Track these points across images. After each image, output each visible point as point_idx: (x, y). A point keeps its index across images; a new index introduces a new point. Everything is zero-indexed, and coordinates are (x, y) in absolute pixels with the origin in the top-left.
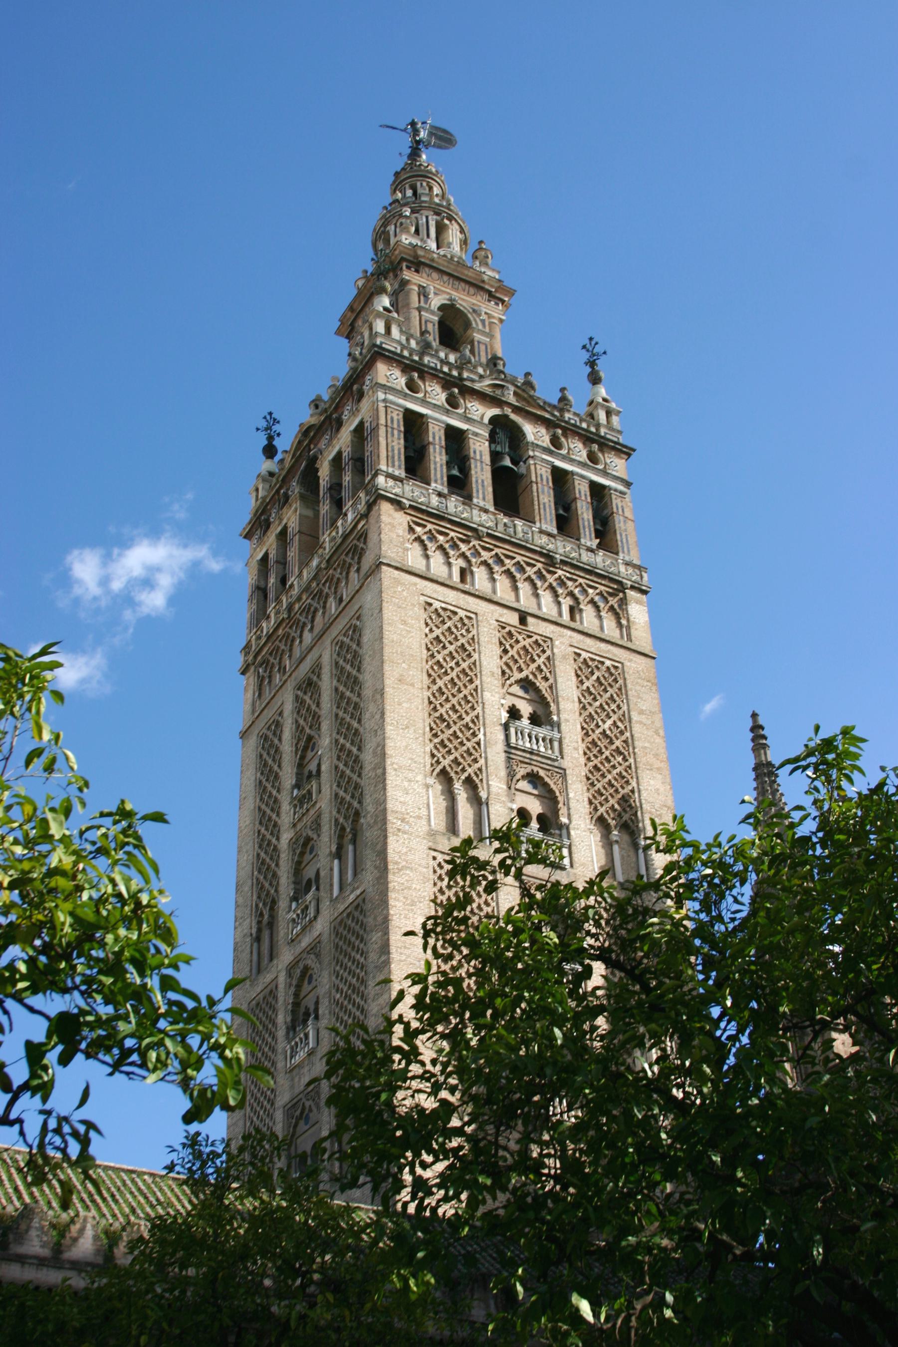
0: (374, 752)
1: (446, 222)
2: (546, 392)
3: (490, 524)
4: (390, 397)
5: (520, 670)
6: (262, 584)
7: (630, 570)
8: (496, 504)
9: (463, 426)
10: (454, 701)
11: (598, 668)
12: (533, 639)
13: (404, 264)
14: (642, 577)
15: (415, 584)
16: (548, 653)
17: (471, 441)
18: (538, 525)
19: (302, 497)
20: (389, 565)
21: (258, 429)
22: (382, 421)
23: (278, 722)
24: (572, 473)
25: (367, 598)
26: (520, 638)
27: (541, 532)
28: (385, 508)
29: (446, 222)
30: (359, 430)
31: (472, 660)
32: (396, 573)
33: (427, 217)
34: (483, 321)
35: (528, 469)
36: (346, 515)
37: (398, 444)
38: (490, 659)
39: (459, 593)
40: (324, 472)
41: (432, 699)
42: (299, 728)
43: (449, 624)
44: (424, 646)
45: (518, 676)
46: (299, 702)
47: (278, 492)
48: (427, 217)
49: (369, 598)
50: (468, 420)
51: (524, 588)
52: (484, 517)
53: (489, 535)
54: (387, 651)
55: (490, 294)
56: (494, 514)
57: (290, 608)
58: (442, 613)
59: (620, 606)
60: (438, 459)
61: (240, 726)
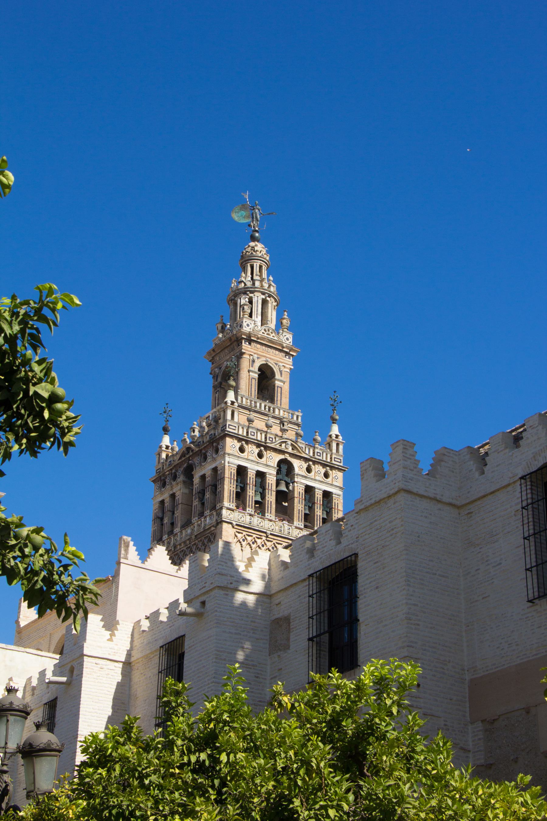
1: (268, 299)
3: (273, 527)
6: (160, 515)
13: (243, 341)
17: (267, 479)
19: (184, 482)
27: (296, 528)
29: (268, 299)
30: (215, 470)
35: (294, 487)
36: (206, 517)
40: (196, 480)
47: (171, 470)
53: (271, 534)
56: (275, 522)
60: (251, 493)
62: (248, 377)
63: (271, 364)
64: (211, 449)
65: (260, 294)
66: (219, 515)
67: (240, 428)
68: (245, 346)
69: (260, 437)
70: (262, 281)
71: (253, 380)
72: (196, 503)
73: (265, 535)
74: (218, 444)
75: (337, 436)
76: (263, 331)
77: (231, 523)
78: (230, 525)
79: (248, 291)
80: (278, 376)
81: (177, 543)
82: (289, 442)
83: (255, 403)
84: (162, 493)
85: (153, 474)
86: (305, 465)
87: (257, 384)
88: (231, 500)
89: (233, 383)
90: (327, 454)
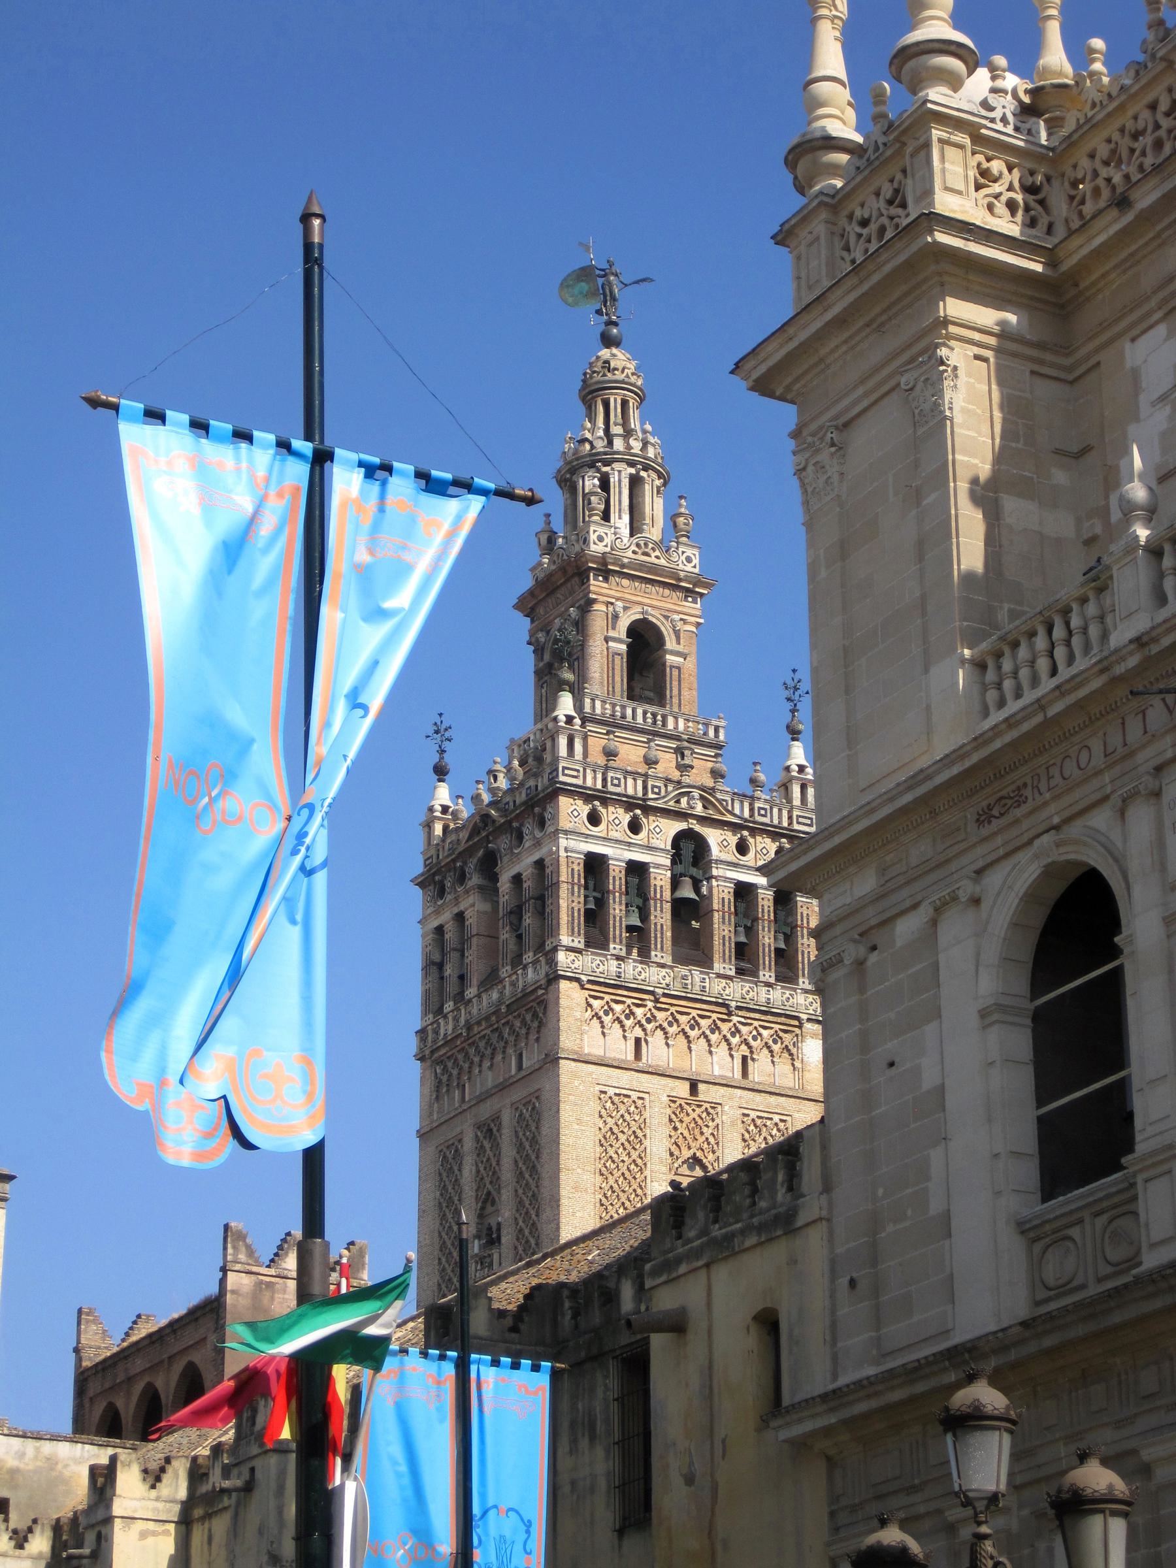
1: (643, 474)
3: (668, 980)
4: (572, 844)
6: (437, 957)
12: (703, 1108)
15: (591, 1074)
16: (717, 1121)
17: (652, 875)
19: (481, 888)
26: (690, 1110)
27: (719, 976)
29: (643, 474)
30: (540, 864)
32: (573, 1064)
33: (620, 472)
35: (710, 889)
36: (525, 967)
41: (604, 1200)
45: (687, 1154)
47: (454, 861)
50: (650, 848)
52: (663, 972)
53: (665, 995)
55: (687, 590)
56: (671, 967)
60: (617, 911)
62: (605, 649)
63: (655, 618)
64: (530, 820)
65: (623, 466)
66: (552, 962)
67: (588, 771)
68: (596, 585)
69: (632, 788)
70: (628, 433)
71: (618, 659)
72: (505, 935)
73: (652, 998)
74: (544, 809)
75: (801, 769)
76: (634, 548)
77: (578, 980)
78: (575, 984)
79: (599, 461)
80: (670, 643)
81: (473, 1021)
82: (696, 794)
83: (623, 707)
84: (437, 912)
85: (418, 868)
86: (733, 840)
87: (625, 665)
88: (576, 929)
89: (569, 676)
90: (780, 810)
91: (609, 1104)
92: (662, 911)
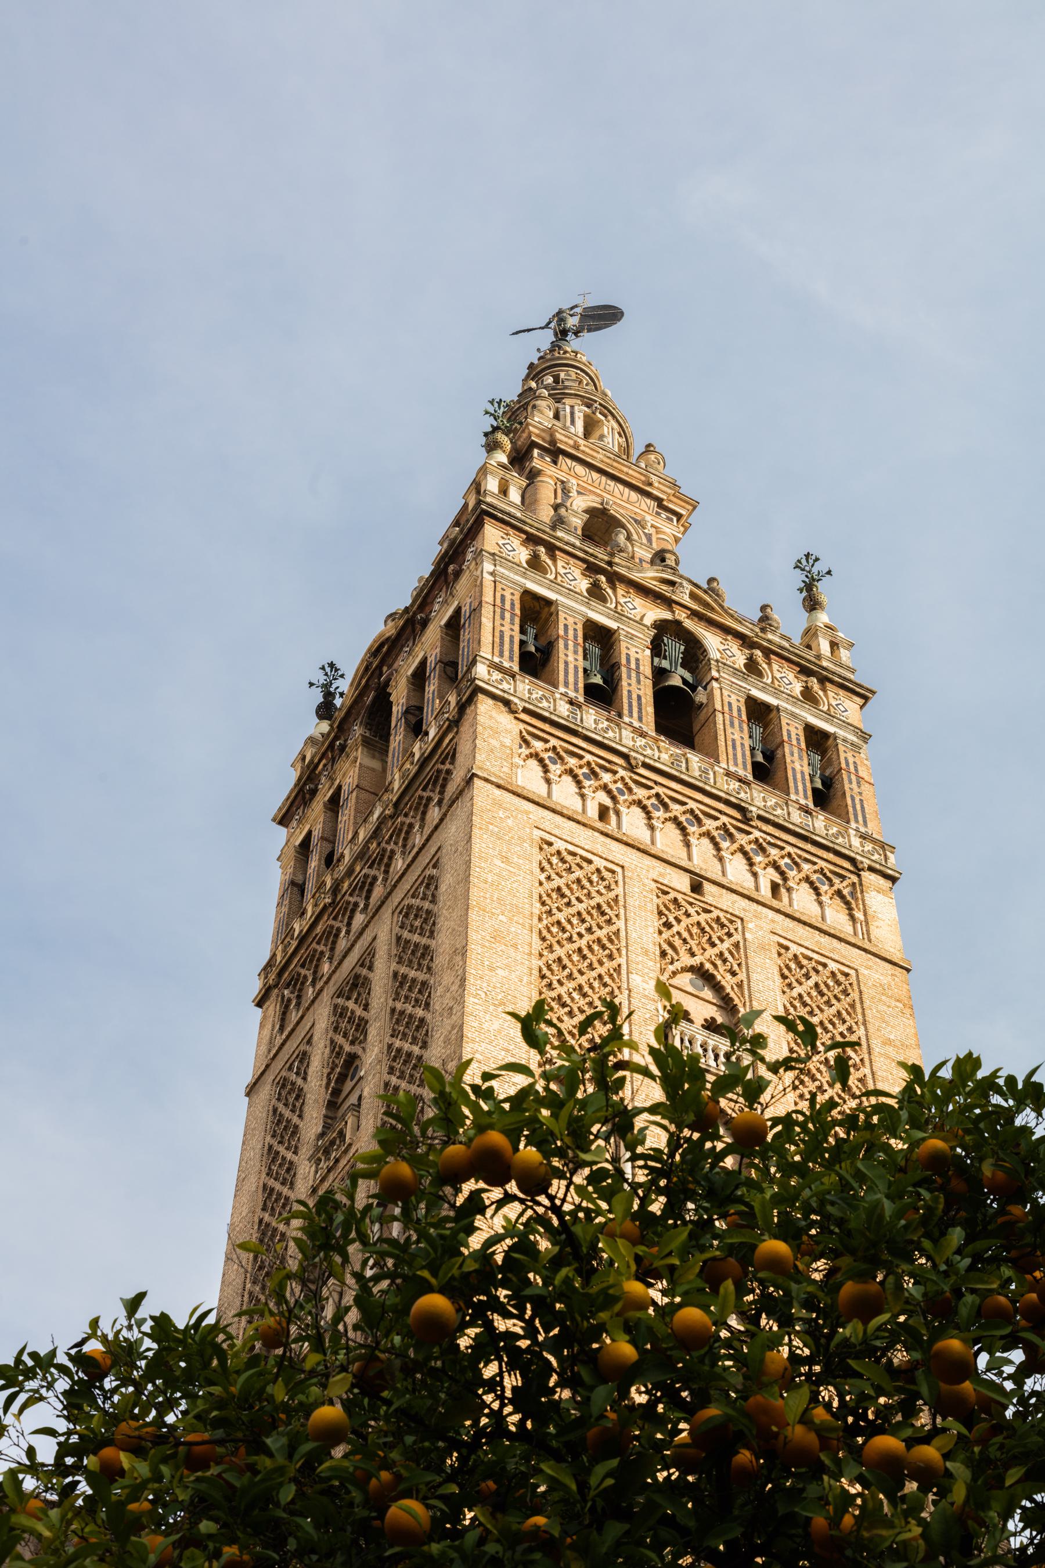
0: (447, 1041)
2: (741, 604)
5: (693, 955)
6: (299, 879)
7: (869, 847)
8: (660, 728)
9: (612, 625)
10: (582, 980)
11: (817, 972)
12: (714, 915)
14: (886, 858)
15: (527, 813)
17: (623, 645)
18: (724, 765)
20: (486, 780)
21: (311, 684)
22: (488, 597)
23: (305, 1053)
24: (778, 708)
25: (452, 831)
26: (691, 911)
27: (728, 774)
28: (484, 706)
31: (614, 928)
32: (498, 792)
33: (572, 407)
34: (649, 537)
35: (711, 696)
37: (512, 630)
38: (641, 930)
39: (596, 834)
40: (400, 696)
41: (545, 970)
42: (335, 1050)
43: (578, 873)
44: (536, 897)
45: (687, 961)
46: (339, 1012)
48: (572, 407)
49: (453, 830)
51: (702, 849)
52: (641, 742)
54: (474, 893)
55: (659, 501)
57: (336, 889)
58: (569, 858)
59: (853, 894)
60: (571, 659)
61: (248, 1078)
77: (507, 703)
88: (507, 653)
91: (555, 860)
92: (639, 682)
